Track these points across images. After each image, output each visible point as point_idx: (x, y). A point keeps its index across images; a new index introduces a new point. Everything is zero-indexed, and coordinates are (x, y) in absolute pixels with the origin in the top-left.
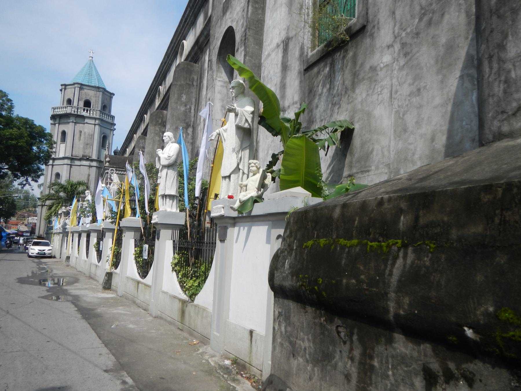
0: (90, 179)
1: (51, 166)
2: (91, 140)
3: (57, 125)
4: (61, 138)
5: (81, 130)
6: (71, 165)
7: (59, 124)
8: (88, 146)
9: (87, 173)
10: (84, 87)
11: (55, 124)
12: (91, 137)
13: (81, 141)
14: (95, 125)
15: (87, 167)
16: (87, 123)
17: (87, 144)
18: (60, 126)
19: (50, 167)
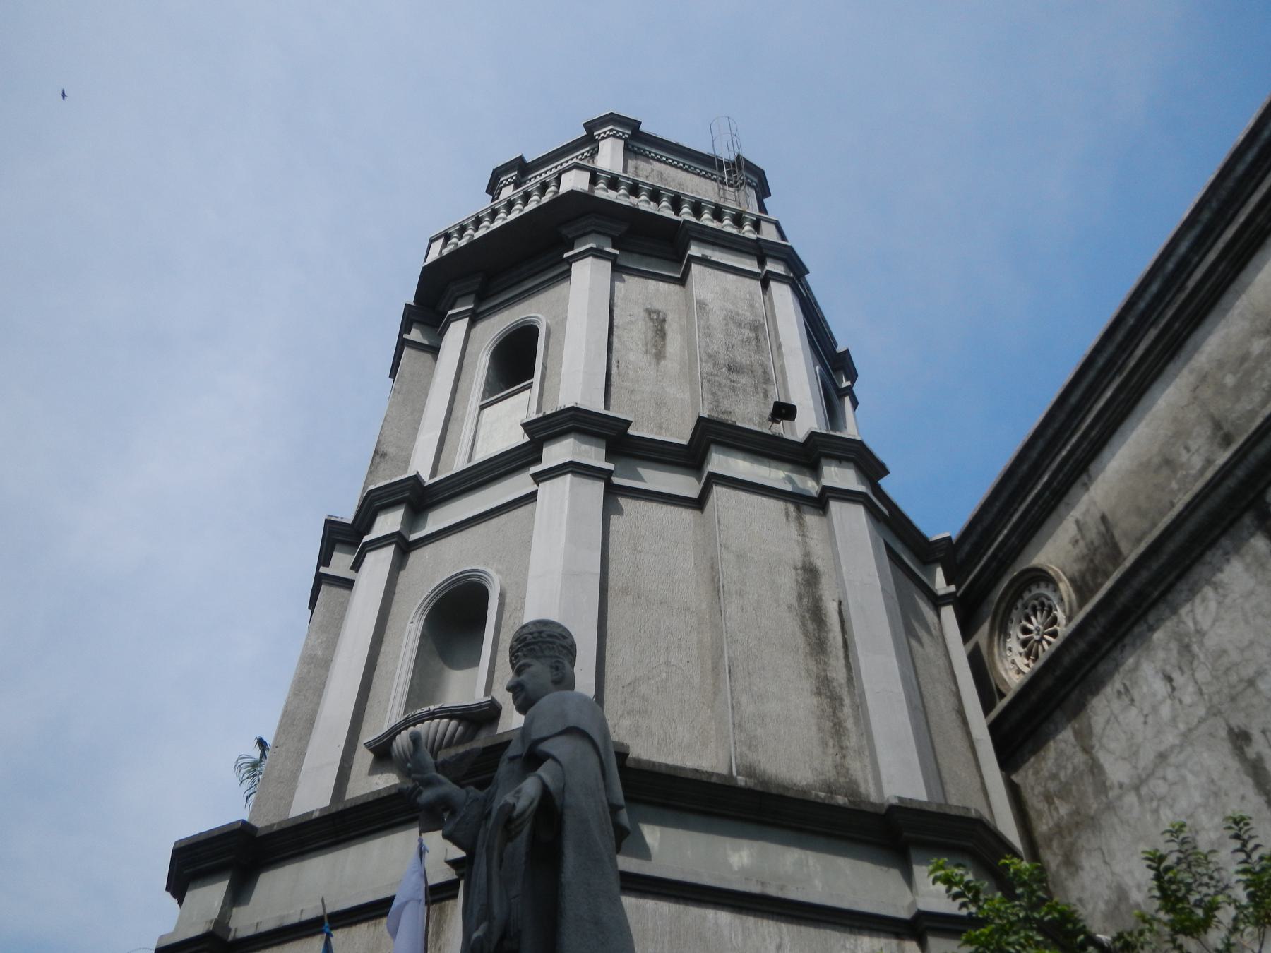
0: (831, 608)
1: (388, 553)
2: (759, 349)
3: (457, 331)
4: (487, 383)
5: (657, 305)
6: (613, 492)
7: (475, 318)
8: (743, 380)
9: (796, 555)
10: (654, 151)
11: (434, 350)
12: (748, 333)
13: (672, 363)
14: (765, 281)
15: (774, 506)
16: (704, 261)
17: (733, 368)
18: (481, 327)
19: (379, 562)
